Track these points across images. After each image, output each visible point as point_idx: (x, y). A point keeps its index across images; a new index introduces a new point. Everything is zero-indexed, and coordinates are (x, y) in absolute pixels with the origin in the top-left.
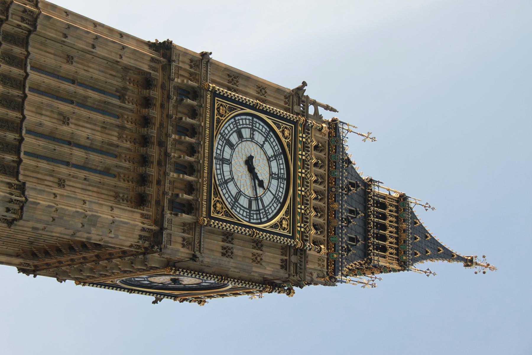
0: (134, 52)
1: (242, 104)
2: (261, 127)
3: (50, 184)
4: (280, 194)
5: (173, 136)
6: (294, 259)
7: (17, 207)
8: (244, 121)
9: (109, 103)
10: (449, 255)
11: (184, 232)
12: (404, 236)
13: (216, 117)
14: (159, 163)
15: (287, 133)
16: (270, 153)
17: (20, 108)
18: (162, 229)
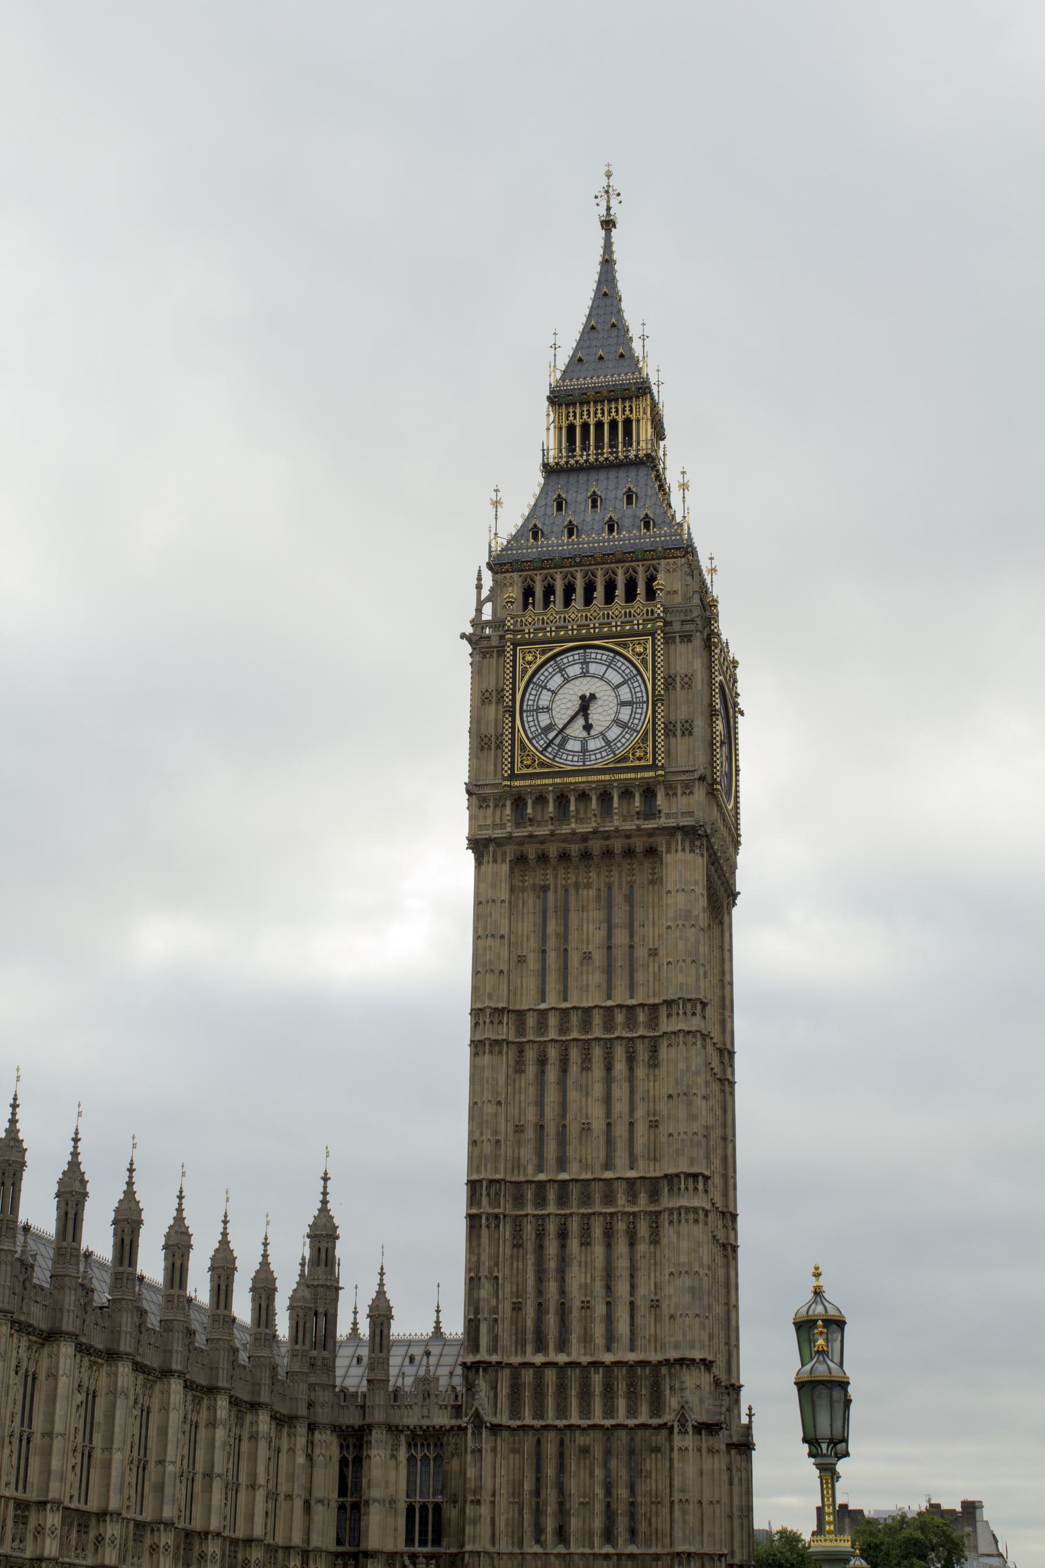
0: (494, 886)
1: (513, 733)
2: (532, 697)
3: (656, 965)
4: (604, 658)
5: (573, 825)
6: (677, 627)
7: (689, 1005)
8: (532, 724)
9: (556, 907)
10: (608, 263)
11: (675, 794)
12: (605, 393)
13: (539, 770)
14: (607, 838)
15: (529, 658)
16: (558, 679)
17: (587, 1011)
18: (679, 828)
